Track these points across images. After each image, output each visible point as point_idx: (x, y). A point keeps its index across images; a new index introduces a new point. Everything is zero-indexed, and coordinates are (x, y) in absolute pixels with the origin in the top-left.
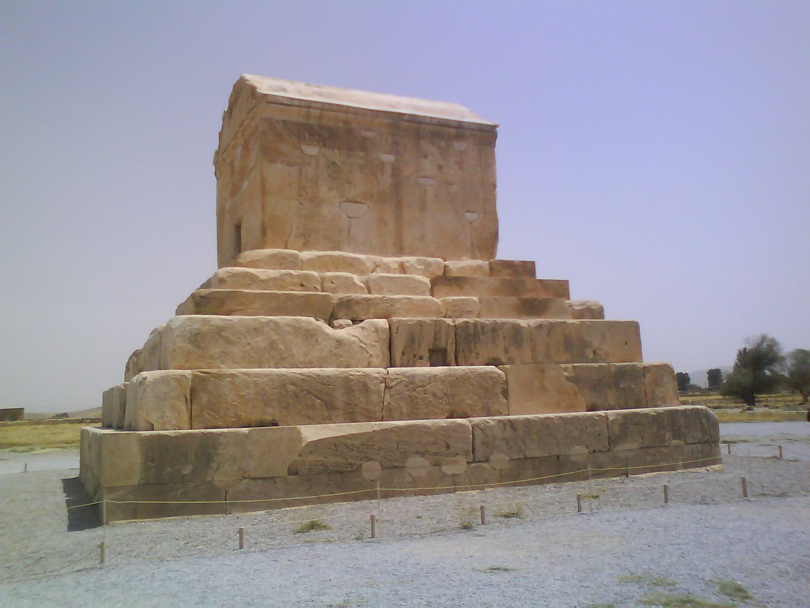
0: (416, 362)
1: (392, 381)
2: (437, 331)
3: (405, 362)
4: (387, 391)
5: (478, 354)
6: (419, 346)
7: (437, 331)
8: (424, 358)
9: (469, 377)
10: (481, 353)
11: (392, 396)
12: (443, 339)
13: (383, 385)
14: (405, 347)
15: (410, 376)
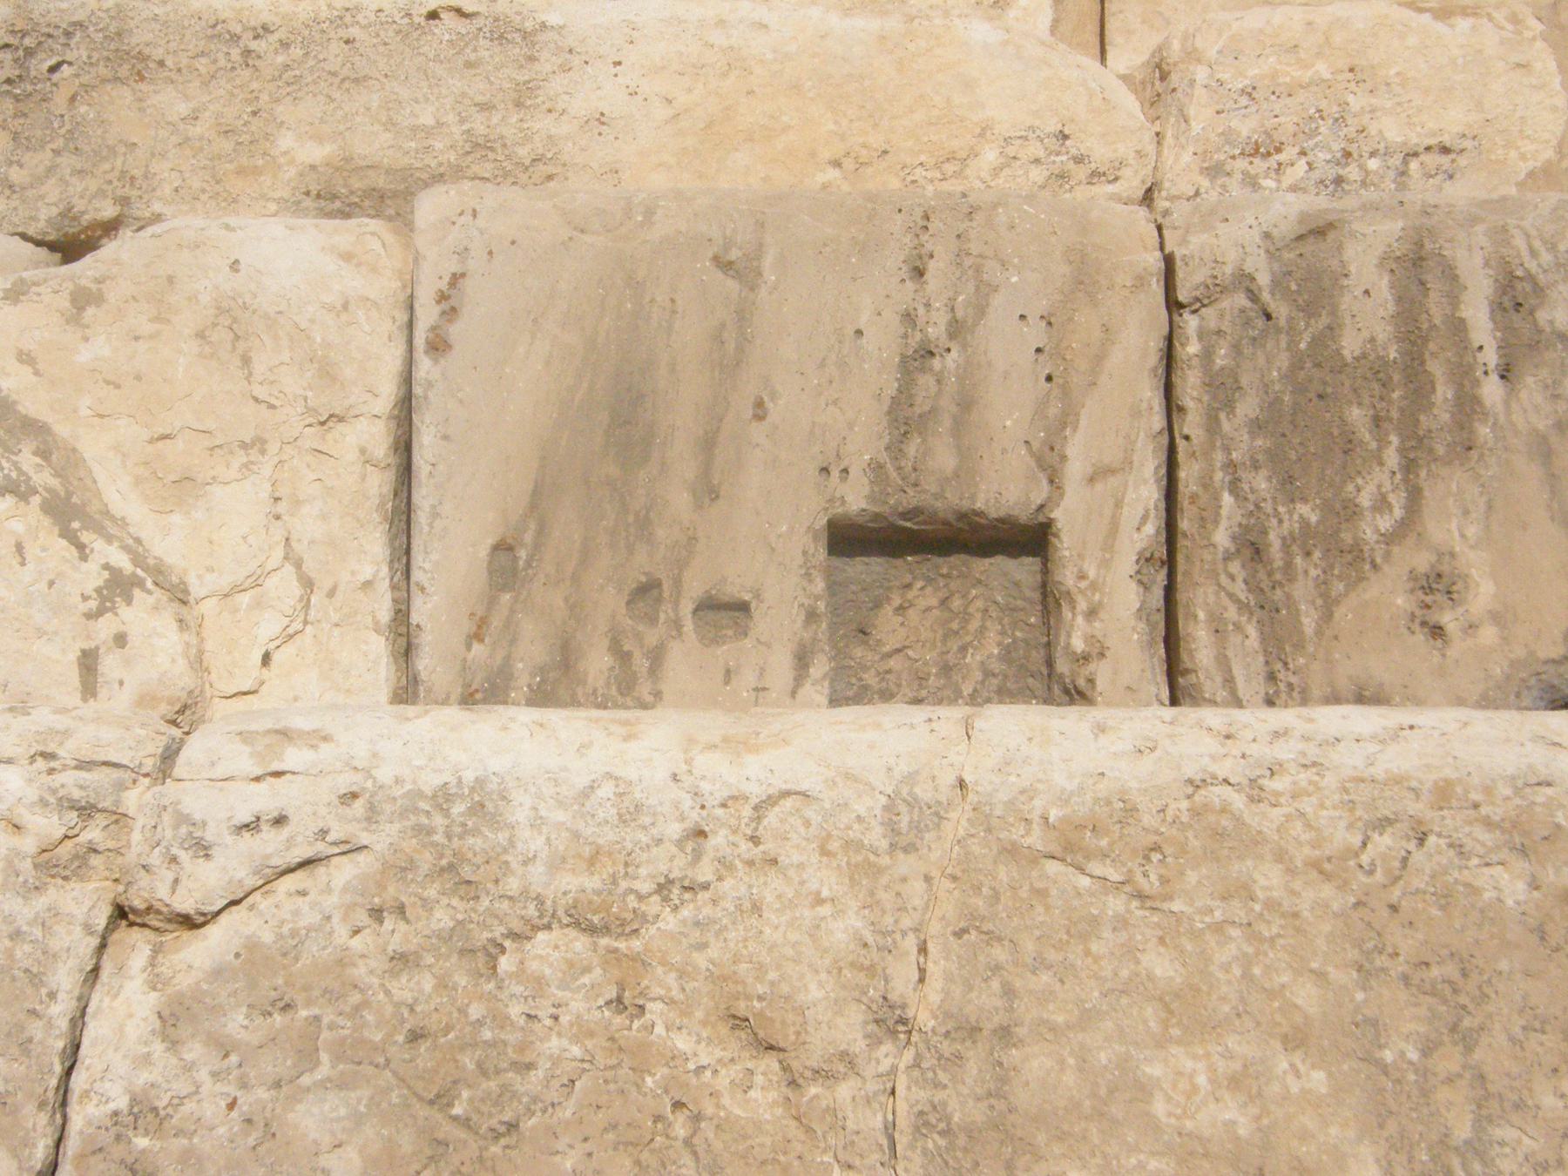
0: (657, 657)
1: (203, 849)
2: (936, 330)
3: (532, 650)
4: (136, 946)
5: (1438, 585)
6: (708, 491)
7: (936, 330)
8: (761, 624)
9: (1223, 837)
10: (1483, 593)
11: (173, 1021)
12: (1009, 413)
13: (85, 902)
14: (538, 501)
15: (443, 798)
